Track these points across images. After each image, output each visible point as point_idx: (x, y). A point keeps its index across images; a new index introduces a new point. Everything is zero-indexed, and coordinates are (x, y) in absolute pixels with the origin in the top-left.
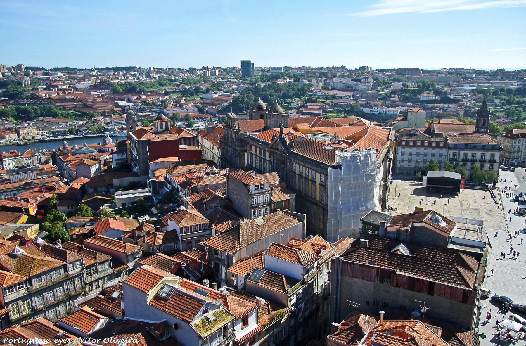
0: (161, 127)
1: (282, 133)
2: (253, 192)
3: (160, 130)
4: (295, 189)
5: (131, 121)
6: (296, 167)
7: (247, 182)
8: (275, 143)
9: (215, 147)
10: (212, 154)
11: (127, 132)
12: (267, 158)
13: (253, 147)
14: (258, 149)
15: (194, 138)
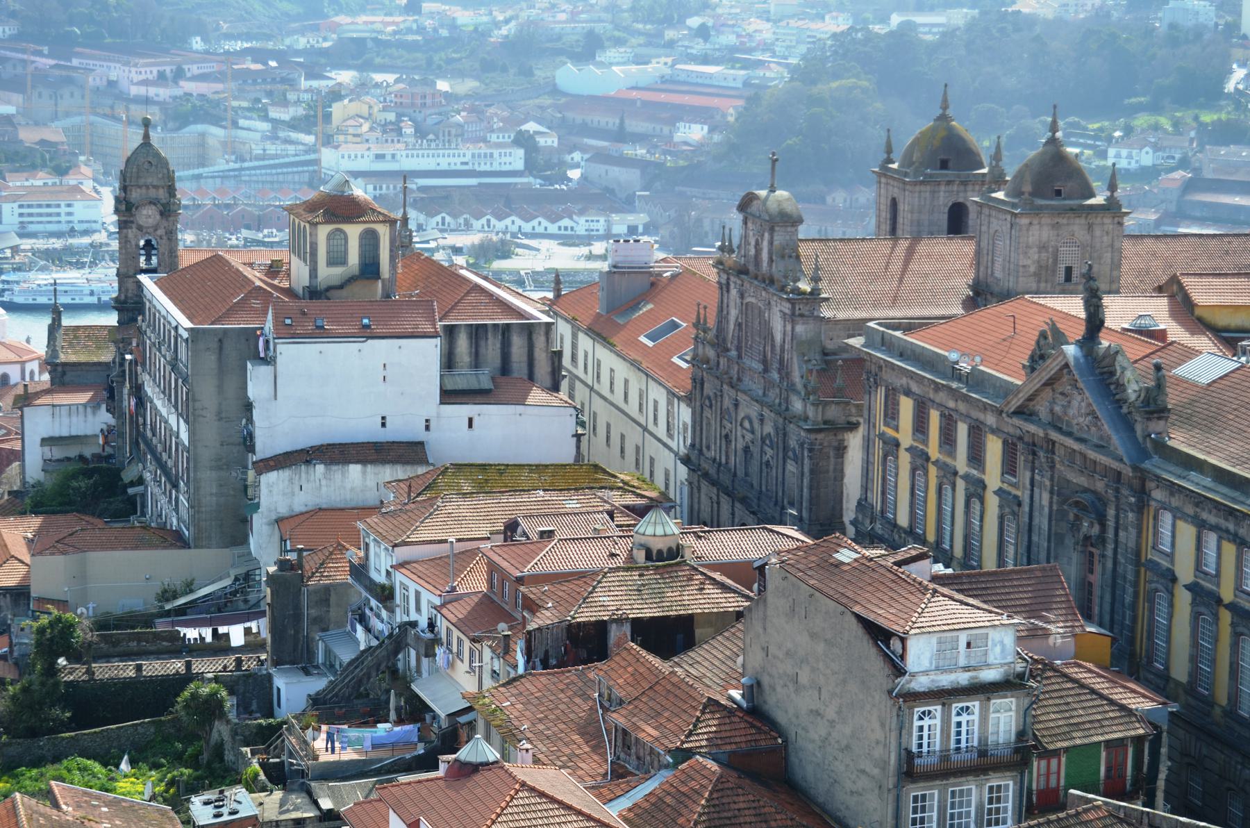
0: (337, 258)
1: (1095, 323)
2: (921, 683)
3: (327, 274)
4: (1165, 676)
5: (148, 216)
6: (1179, 543)
7: (884, 616)
8: (1050, 383)
9: (657, 394)
10: (634, 437)
11: (127, 276)
12: (993, 476)
13: (906, 407)
14: (934, 417)
15: (529, 330)
